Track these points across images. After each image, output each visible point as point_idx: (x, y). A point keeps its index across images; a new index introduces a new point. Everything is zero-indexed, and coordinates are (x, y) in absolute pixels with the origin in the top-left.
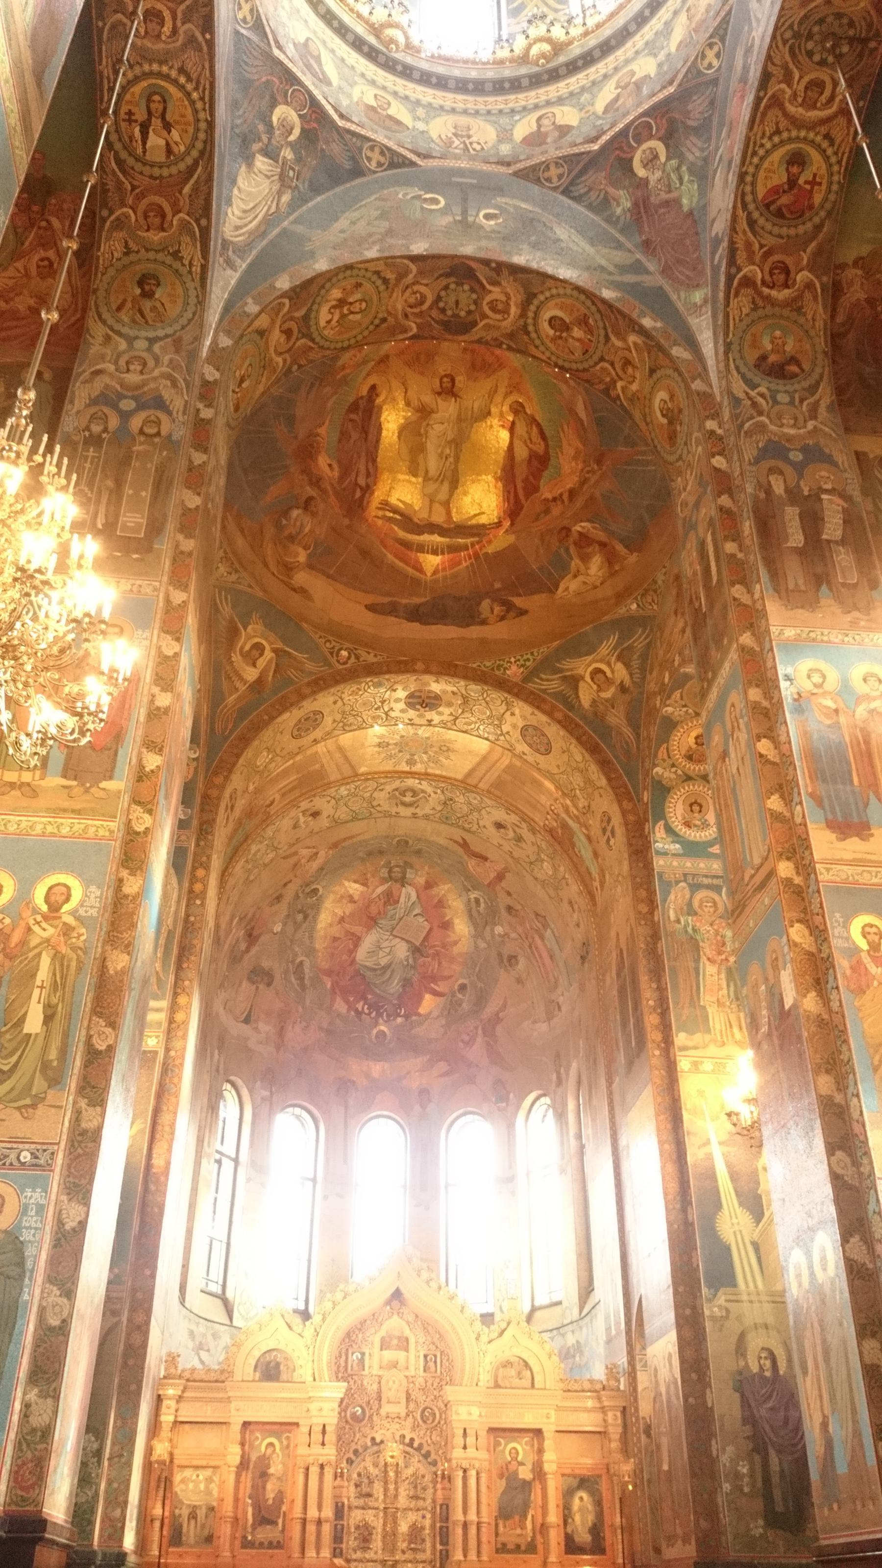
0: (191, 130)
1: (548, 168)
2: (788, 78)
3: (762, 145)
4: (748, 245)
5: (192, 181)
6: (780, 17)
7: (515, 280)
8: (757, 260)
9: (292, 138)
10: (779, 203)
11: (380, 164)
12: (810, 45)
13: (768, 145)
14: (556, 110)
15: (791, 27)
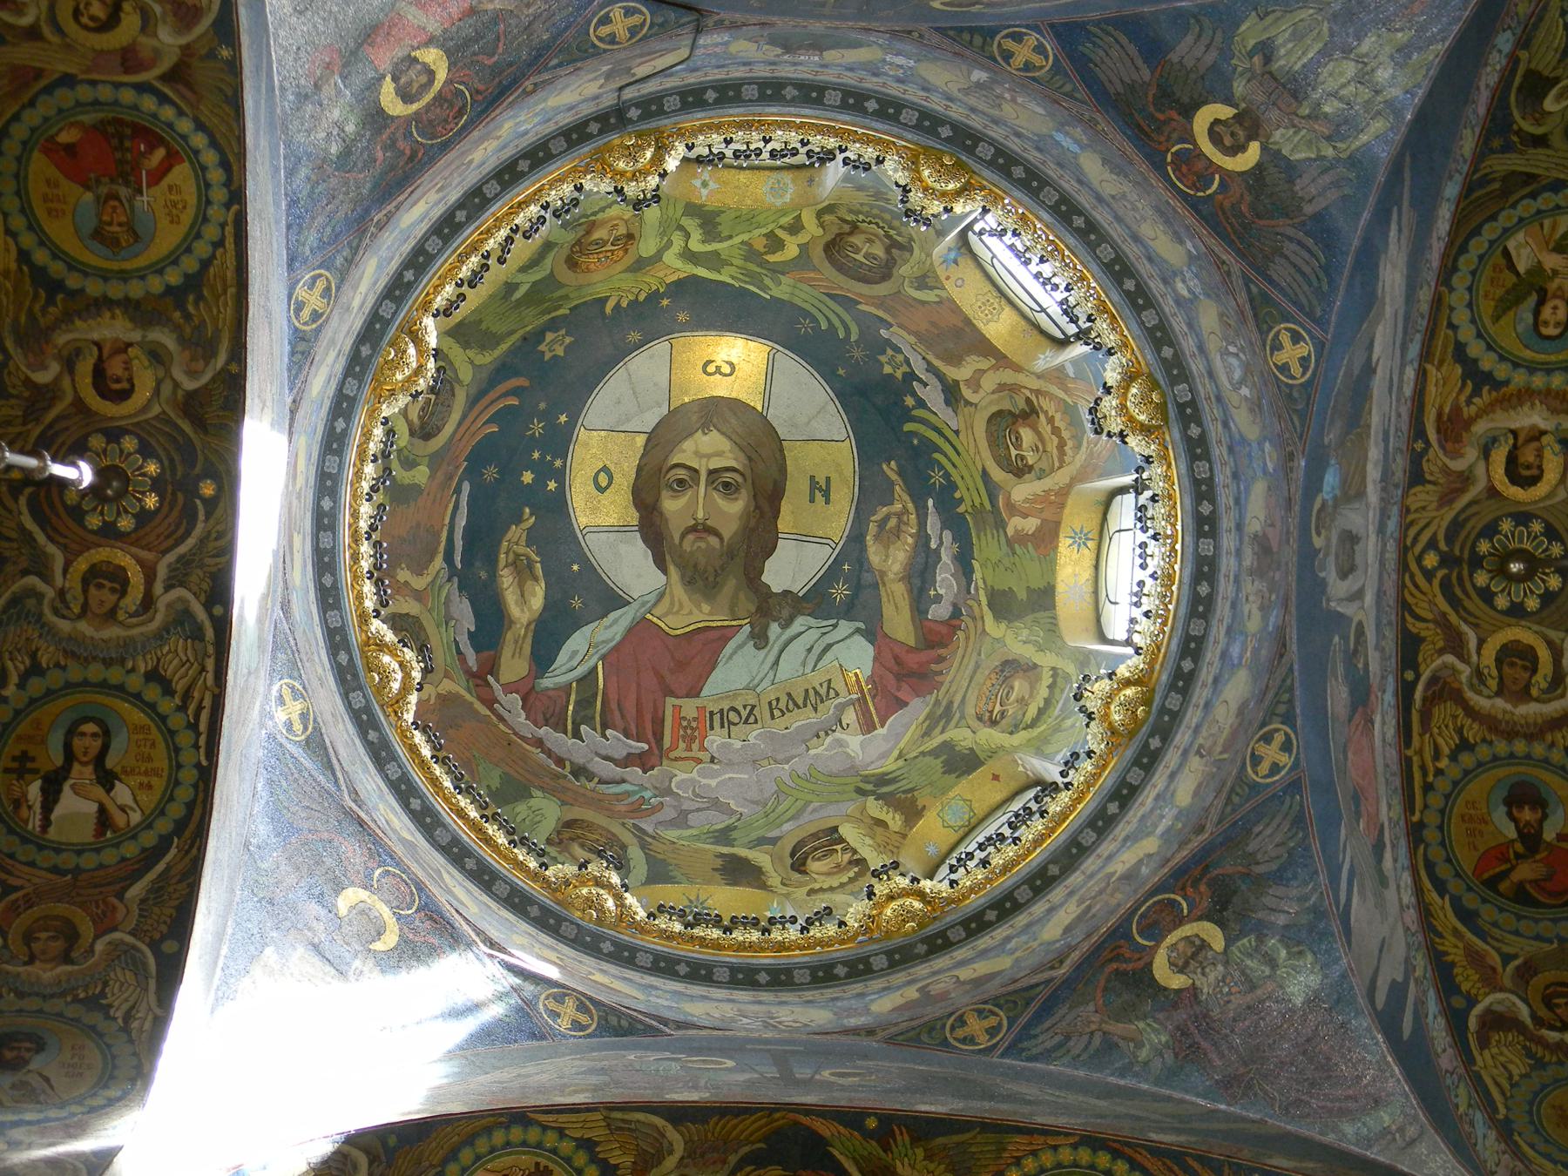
0: (159, 784)
1: (961, 1021)
2: (1455, 644)
3: (1439, 772)
4: (1475, 958)
5: (151, 875)
6: (1405, 527)
7: (929, 1157)
8: (1507, 982)
9: (378, 946)
10: (1516, 876)
11: (577, 1026)
12: (1481, 579)
13: (1455, 772)
14: (956, 972)
15: (1432, 544)
